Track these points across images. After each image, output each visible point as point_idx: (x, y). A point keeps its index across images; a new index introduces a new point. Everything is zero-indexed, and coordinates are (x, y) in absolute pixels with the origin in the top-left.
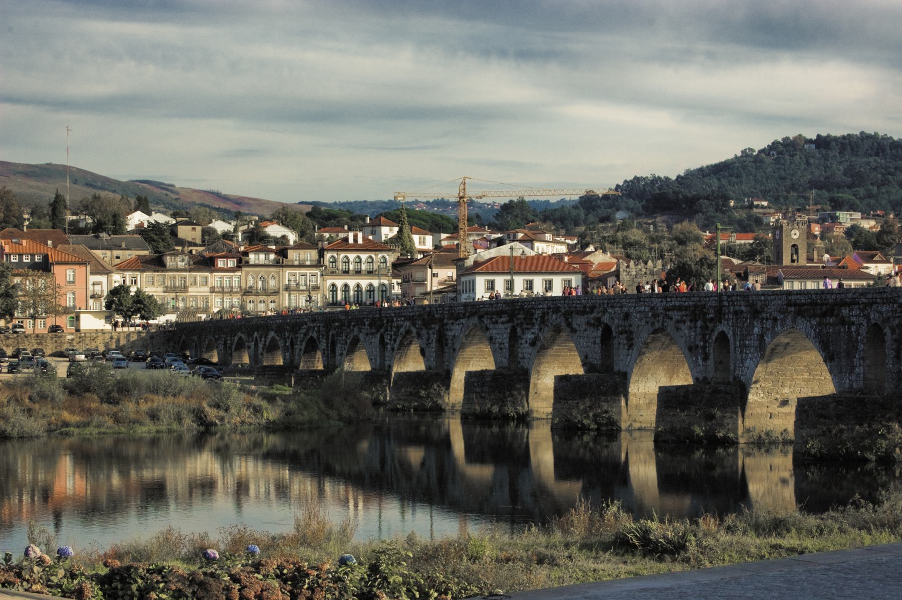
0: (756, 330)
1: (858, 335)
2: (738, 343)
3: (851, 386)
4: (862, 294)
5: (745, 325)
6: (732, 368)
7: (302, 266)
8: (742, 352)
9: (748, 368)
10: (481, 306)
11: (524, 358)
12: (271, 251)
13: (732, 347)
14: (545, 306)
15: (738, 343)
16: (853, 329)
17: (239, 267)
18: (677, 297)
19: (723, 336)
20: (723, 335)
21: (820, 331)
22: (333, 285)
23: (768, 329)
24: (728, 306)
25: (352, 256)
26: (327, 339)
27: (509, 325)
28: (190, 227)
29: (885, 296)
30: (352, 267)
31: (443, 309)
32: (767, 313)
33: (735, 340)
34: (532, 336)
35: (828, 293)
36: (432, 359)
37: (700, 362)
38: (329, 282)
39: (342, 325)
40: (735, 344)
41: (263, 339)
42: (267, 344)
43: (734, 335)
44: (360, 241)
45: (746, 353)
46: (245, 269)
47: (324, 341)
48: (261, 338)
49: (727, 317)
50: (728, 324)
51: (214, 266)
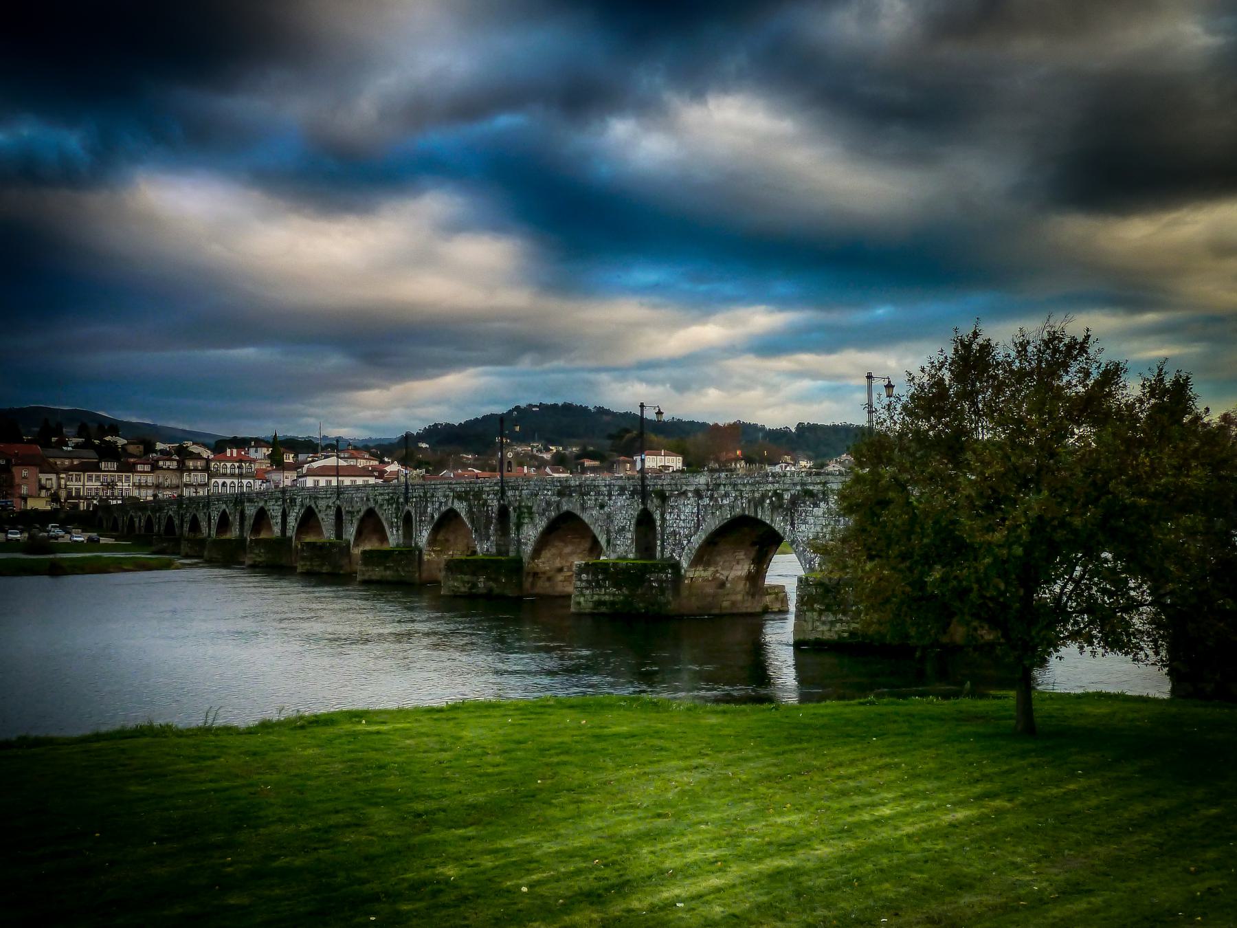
6: (414, 536)
7: (196, 470)
8: (420, 525)
13: (414, 522)
16: (490, 508)
20: (409, 513)
25: (229, 465)
26: (179, 516)
30: (229, 471)
34: (295, 514)
38: (213, 480)
44: (235, 455)
46: (158, 472)
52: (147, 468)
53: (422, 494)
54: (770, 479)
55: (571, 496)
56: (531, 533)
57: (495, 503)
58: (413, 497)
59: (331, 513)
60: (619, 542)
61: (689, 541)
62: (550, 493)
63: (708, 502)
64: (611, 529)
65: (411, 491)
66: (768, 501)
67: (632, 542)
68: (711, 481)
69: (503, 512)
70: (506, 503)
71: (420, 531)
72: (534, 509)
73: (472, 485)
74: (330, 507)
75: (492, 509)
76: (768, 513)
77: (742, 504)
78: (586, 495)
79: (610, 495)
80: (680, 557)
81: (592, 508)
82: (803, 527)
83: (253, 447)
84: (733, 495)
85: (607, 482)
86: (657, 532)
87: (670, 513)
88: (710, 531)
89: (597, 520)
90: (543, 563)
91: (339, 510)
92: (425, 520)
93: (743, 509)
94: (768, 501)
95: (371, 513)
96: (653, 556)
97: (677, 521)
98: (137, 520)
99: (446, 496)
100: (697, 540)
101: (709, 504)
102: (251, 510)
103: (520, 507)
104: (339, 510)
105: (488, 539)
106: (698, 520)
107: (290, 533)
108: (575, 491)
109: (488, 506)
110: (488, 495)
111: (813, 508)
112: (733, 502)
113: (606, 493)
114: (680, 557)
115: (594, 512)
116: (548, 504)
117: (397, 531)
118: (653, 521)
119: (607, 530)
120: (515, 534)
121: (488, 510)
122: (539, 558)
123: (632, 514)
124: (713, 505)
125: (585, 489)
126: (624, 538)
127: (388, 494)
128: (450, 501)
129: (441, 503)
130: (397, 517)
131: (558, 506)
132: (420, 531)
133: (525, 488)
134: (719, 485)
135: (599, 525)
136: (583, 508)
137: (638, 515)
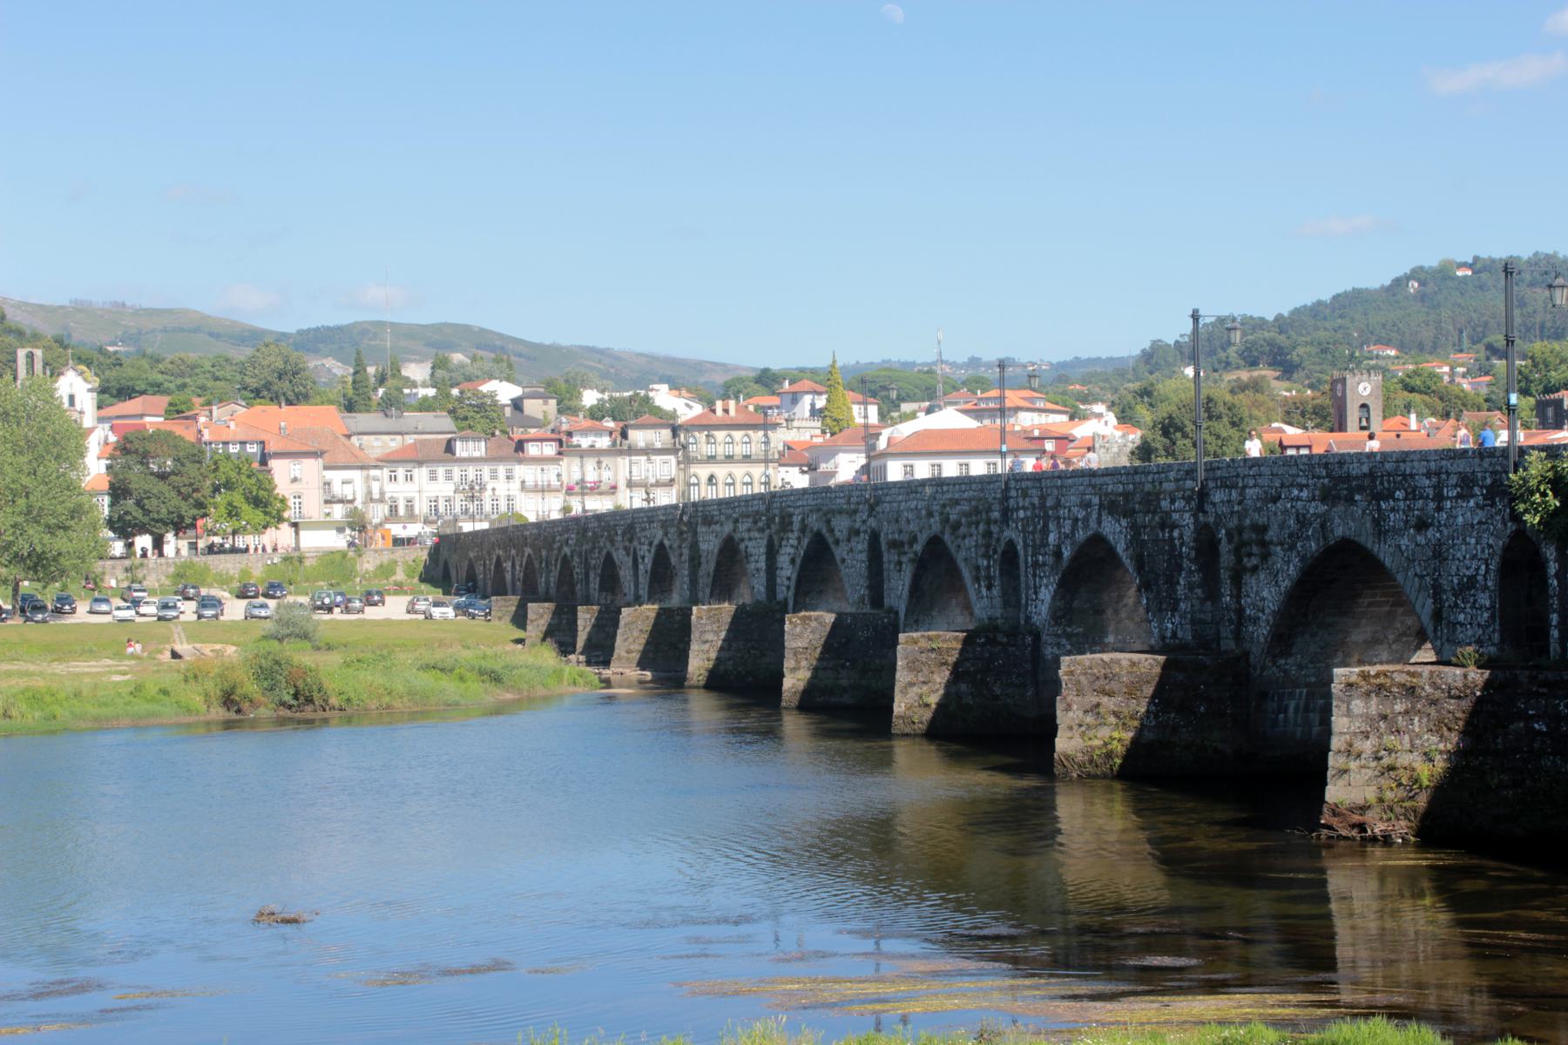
1: (1182, 545)
2: (1030, 559)
5: (1039, 527)
6: (1023, 602)
8: (1034, 575)
9: (1043, 601)
15: (1030, 559)
17: (615, 451)
18: (954, 485)
20: (1011, 544)
24: (1017, 497)
27: (767, 532)
29: (1219, 473)
32: (1065, 508)
33: (1026, 556)
35: (1143, 473)
36: (686, 587)
37: (984, 591)
40: (1026, 563)
43: (1026, 546)
50: (1017, 527)
51: (523, 451)
52: (550, 449)
53: (1036, 501)
55: (1353, 502)
57: (1188, 519)
58: (1018, 509)
59: (860, 547)
60: (1461, 617)
62: (1304, 494)
67: (1493, 617)
69: (1207, 544)
70: (1211, 519)
71: (1035, 587)
72: (1272, 534)
73: (1137, 478)
74: (857, 533)
75: (1181, 536)
78: (1386, 499)
79: (1439, 498)
81: (1397, 532)
85: (1433, 465)
89: (1411, 561)
90: (1300, 667)
91: (874, 537)
92: (1044, 564)
95: (935, 542)
98: (508, 565)
99: (1086, 505)
102: (710, 544)
103: (1240, 530)
104: (874, 537)
105: (1175, 609)
108: (1361, 489)
109: (1171, 532)
110: (1173, 501)
113: (1431, 492)
115: (1404, 542)
116: (1302, 521)
117: (989, 588)
118: (1542, 565)
119: (1434, 587)
120: (1231, 596)
121: (1172, 539)
122: (1286, 653)
123: (1490, 546)
125: (1382, 483)
126: (1473, 607)
127: (969, 500)
128: (1094, 516)
130: (986, 556)
131: (1323, 526)
132: (1035, 587)
133: (1251, 482)
135: (1416, 575)
136: (1380, 531)
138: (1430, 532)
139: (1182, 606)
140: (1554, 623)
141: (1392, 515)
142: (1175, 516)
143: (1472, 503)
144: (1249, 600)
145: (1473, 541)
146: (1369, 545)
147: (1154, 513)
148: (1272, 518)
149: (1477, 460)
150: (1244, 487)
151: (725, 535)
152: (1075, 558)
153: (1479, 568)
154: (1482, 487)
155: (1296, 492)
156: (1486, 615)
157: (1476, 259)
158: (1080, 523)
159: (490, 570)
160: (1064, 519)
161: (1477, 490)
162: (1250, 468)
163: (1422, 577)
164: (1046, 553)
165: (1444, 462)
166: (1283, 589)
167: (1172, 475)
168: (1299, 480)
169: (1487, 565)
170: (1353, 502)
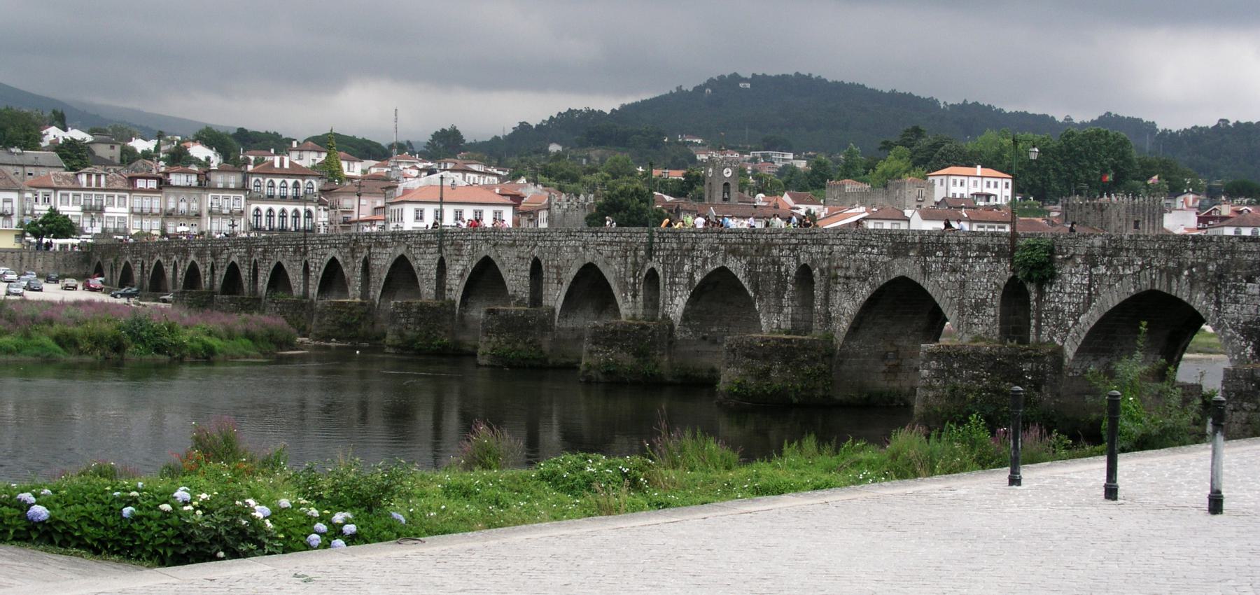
0: (686, 268)
1: (787, 276)
2: (668, 280)
3: (779, 327)
4: (792, 235)
5: (676, 262)
6: (661, 305)
7: (226, 189)
8: (671, 290)
9: (677, 305)
10: (409, 236)
11: (451, 290)
12: (192, 172)
14: (474, 237)
15: (668, 280)
16: (783, 269)
17: (159, 189)
18: (608, 233)
19: (652, 275)
21: (750, 271)
22: (258, 210)
23: (698, 267)
24: (659, 243)
25: (278, 181)
26: (250, 265)
27: (438, 256)
28: (109, 146)
30: (277, 192)
31: (370, 238)
32: (698, 251)
33: (665, 277)
34: (461, 268)
37: (630, 298)
38: (254, 206)
39: (265, 251)
41: (183, 263)
42: (187, 268)
43: (665, 272)
44: (286, 165)
45: (676, 291)
46: (166, 190)
47: (246, 267)
48: (180, 261)
49: (657, 253)
50: (658, 260)
52: (153, 184)
54: (1191, 244)
55: (907, 256)
56: (846, 306)
59: (523, 268)
60: (976, 320)
61: (1076, 322)
62: (875, 251)
63: (1104, 270)
64: (966, 301)
65: (656, 240)
66: (1186, 273)
67: (995, 320)
68: (1109, 244)
69: (805, 273)
75: (787, 271)
76: (1186, 287)
77: (1151, 274)
79: (965, 258)
80: (1063, 342)
82: (1231, 308)
83: (295, 150)
84: (1140, 263)
86: (1031, 308)
87: (1051, 284)
88: (1107, 310)
93: (1153, 282)
94: (1186, 273)
96: (1024, 340)
97: (1061, 295)
99: (714, 249)
100: (1089, 319)
101: (1106, 273)
106: (1090, 294)
107: (376, 293)
110: (781, 250)
111: (1246, 283)
112: (1139, 272)
114: (1063, 342)
115: (941, 280)
117: (634, 296)
118: (1027, 294)
119: (959, 304)
123: (995, 284)
124: (1111, 274)
129: (705, 260)
132: (671, 297)
133: (838, 242)
134: (1121, 249)
136: (926, 272)
137: (1006, 286)
138: (958, 275)
139: (785, 310)
140: (1033, 324)
141: (934, 266)
142: (783, 259)
143: (985, 260)
144: (834, 308)
145: (985, 280)
146: (918, 281)
147: (768, 256)
148: (852, 263)
149: (990, 238)
150: (833, 245)
151: (397, 256)
152: (702, 281)
153: (988, 295)
154: (992, 252)
155: (869, 249)
156: (991, 320)
157: (754, 75)
158: (709, 260)
159: (148, 272)
160: (697, 257)
161: (989, 254)
162: (838, 235)
163: (952, 298)
164: (681, 277)
165: (969, 238)
166: (858, 302)
167: (780, 235)
168: (872, 243)
169: (993, 293)
170: (907, 256)
